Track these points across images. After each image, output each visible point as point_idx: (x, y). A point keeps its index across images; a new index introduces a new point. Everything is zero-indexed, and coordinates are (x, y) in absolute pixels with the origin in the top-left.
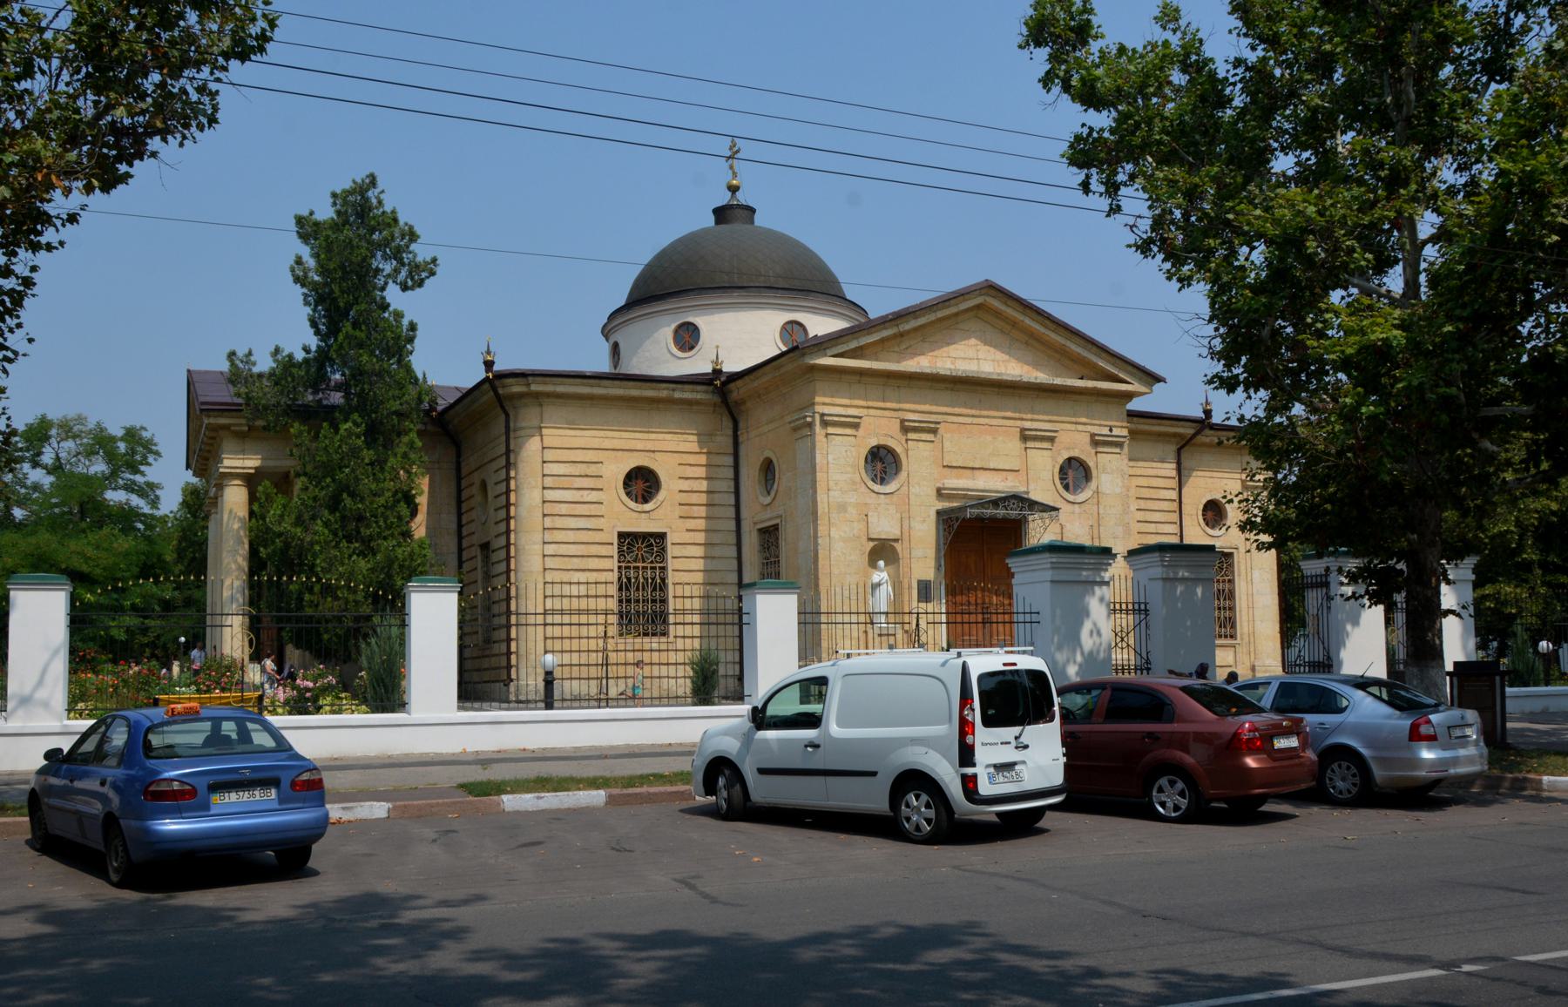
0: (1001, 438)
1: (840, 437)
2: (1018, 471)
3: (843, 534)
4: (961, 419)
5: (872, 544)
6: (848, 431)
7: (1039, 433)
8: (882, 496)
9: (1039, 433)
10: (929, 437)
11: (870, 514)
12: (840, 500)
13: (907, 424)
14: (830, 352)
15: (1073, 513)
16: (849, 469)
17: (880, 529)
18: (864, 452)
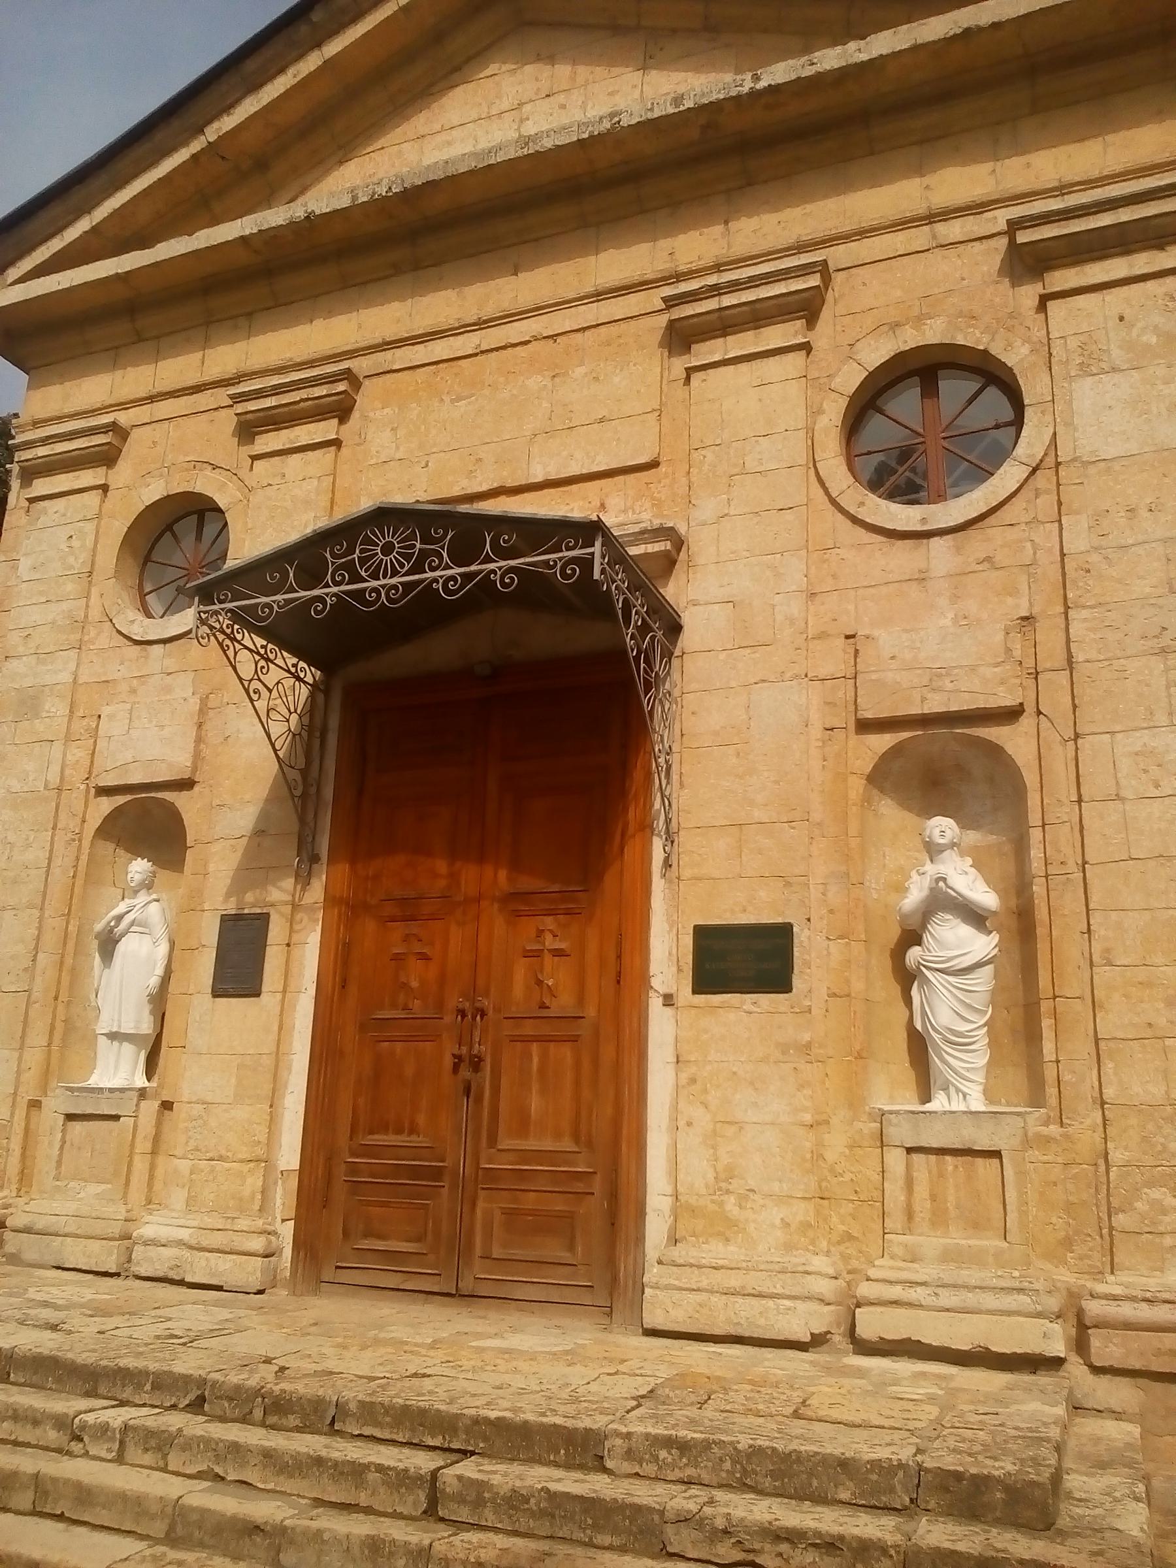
0: (580, 371)
1: (60, 503)
2: (654, 465)
3: (16, 786)
4: (440, 349)
5: (106, 805)
6: (87, 477)
7: (728, 300)
8: (157, 649)
9: (728, 300)
10: (326, 429)
11: (106, 711)
12: (28, 682)
13: (240, 408)
14: (13, 273)
15: (922, 579)
16: (70, 587)
17: (128, 756)
18: (119, 527)
